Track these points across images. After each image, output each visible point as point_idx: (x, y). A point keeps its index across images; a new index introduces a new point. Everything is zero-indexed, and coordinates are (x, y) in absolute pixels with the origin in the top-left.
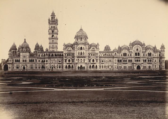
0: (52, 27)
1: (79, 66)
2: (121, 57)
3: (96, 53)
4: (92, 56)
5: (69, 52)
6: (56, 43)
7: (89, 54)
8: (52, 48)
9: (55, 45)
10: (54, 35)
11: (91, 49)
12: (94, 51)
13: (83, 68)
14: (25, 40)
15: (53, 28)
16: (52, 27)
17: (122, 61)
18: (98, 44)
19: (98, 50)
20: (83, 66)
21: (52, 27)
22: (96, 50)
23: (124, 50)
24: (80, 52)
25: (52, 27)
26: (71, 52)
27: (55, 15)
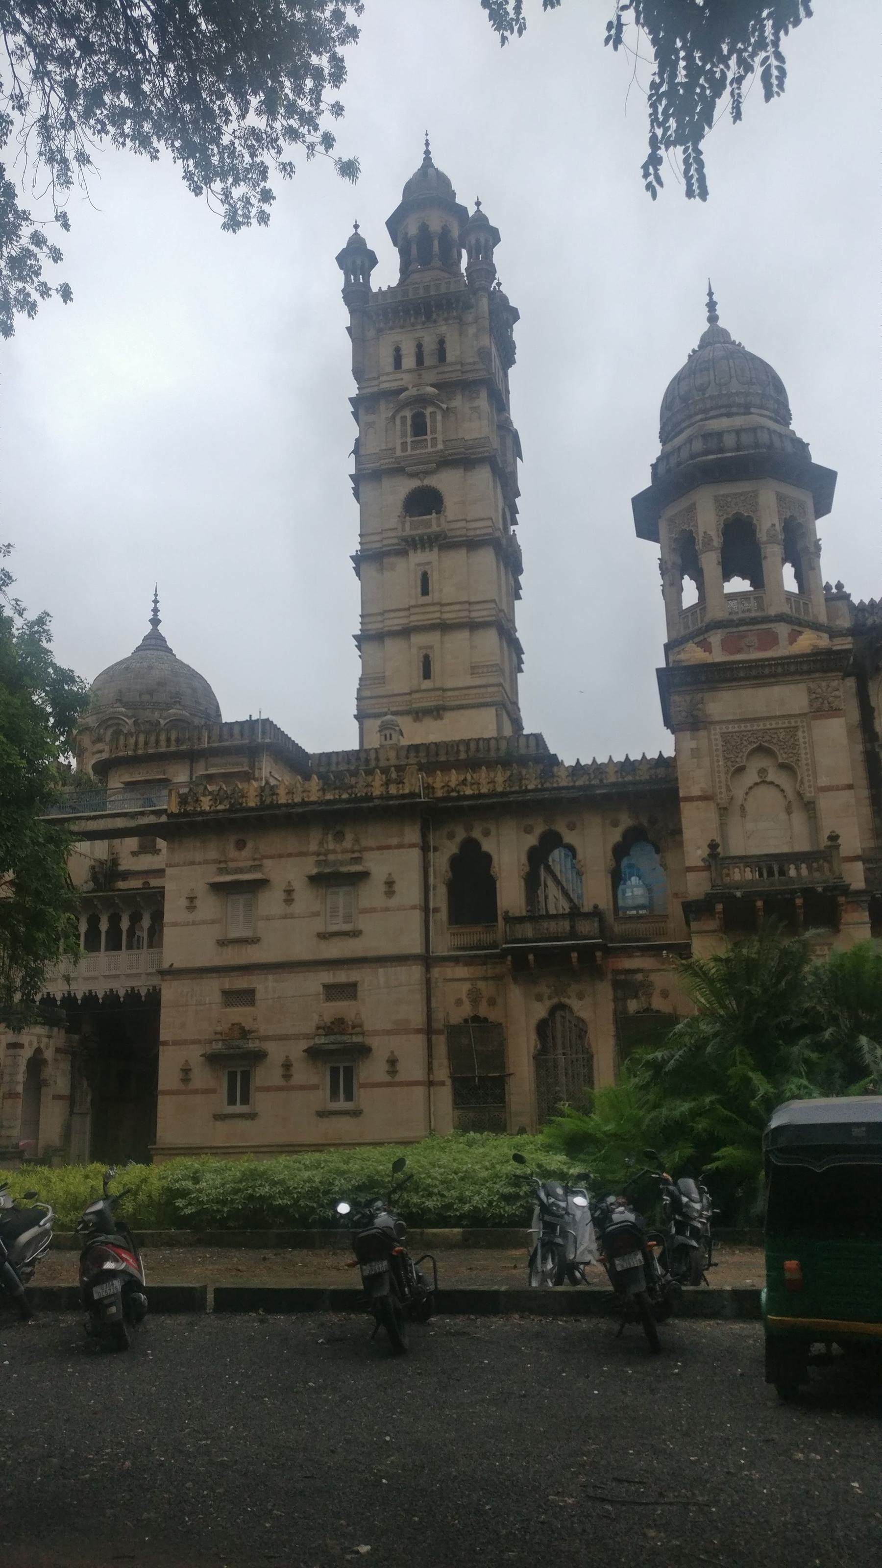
0: (398, 364)
6: (479, 614)
8: (418, 715)
15: (430, 377)
16: (398, 364)
21: (409, 362)
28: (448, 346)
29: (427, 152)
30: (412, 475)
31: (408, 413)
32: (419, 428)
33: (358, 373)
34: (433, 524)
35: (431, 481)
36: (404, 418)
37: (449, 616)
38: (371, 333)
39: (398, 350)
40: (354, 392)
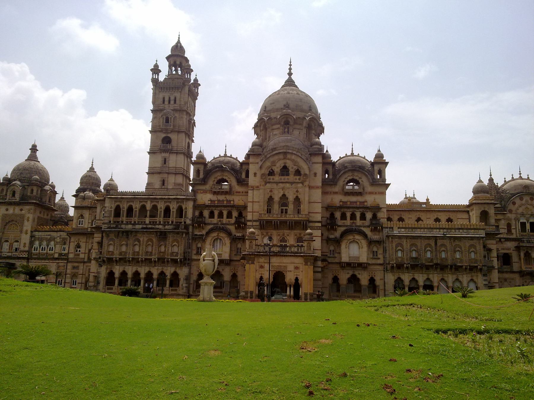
0: (164, 103)
1: (261, 278)
2: (507, 240)
3: (369, 204)
4: (348, 222)
5: (221, 197)
7: (330, 209)
9: (172, 180)
10: (173, 136)
11: (341, 183)
12: (360, 194)
13: (290, 291)
14: (34, 149)
16: (164, 103)
17: (515, 258)
18: (379, 156)
19: (380, 189)
20: (290, 278)
21: (166, 103)
22: (369, 189)
23: (521, 199)
24: (277, 198)
25: (166, 103)
26: (229, 197)
27: (186, 56)
28: (177, 99)
29: (179, 38)
30: (164, 133)
31: (165, 117)
32: (167, 121)
33: (154, 103)
34: (169, 147)
35: (169, 135)
36: (163, 118)
37: (171, 171)
38: (157, 92)
39: (164, 98)
40: (151, 107)
